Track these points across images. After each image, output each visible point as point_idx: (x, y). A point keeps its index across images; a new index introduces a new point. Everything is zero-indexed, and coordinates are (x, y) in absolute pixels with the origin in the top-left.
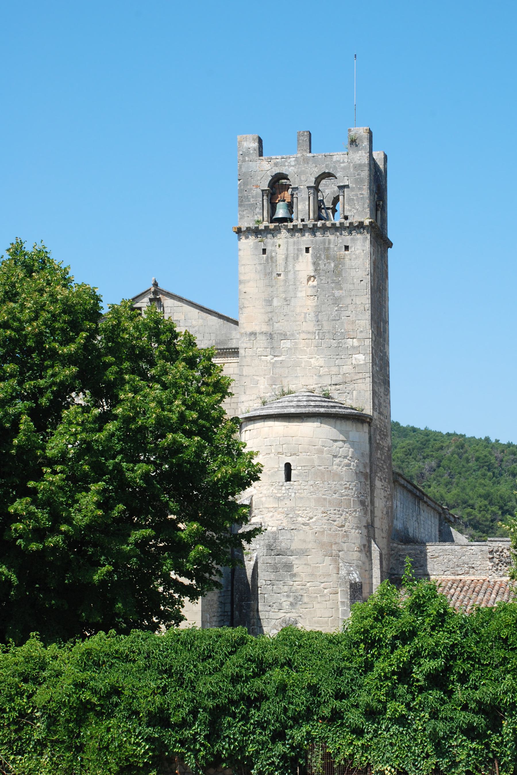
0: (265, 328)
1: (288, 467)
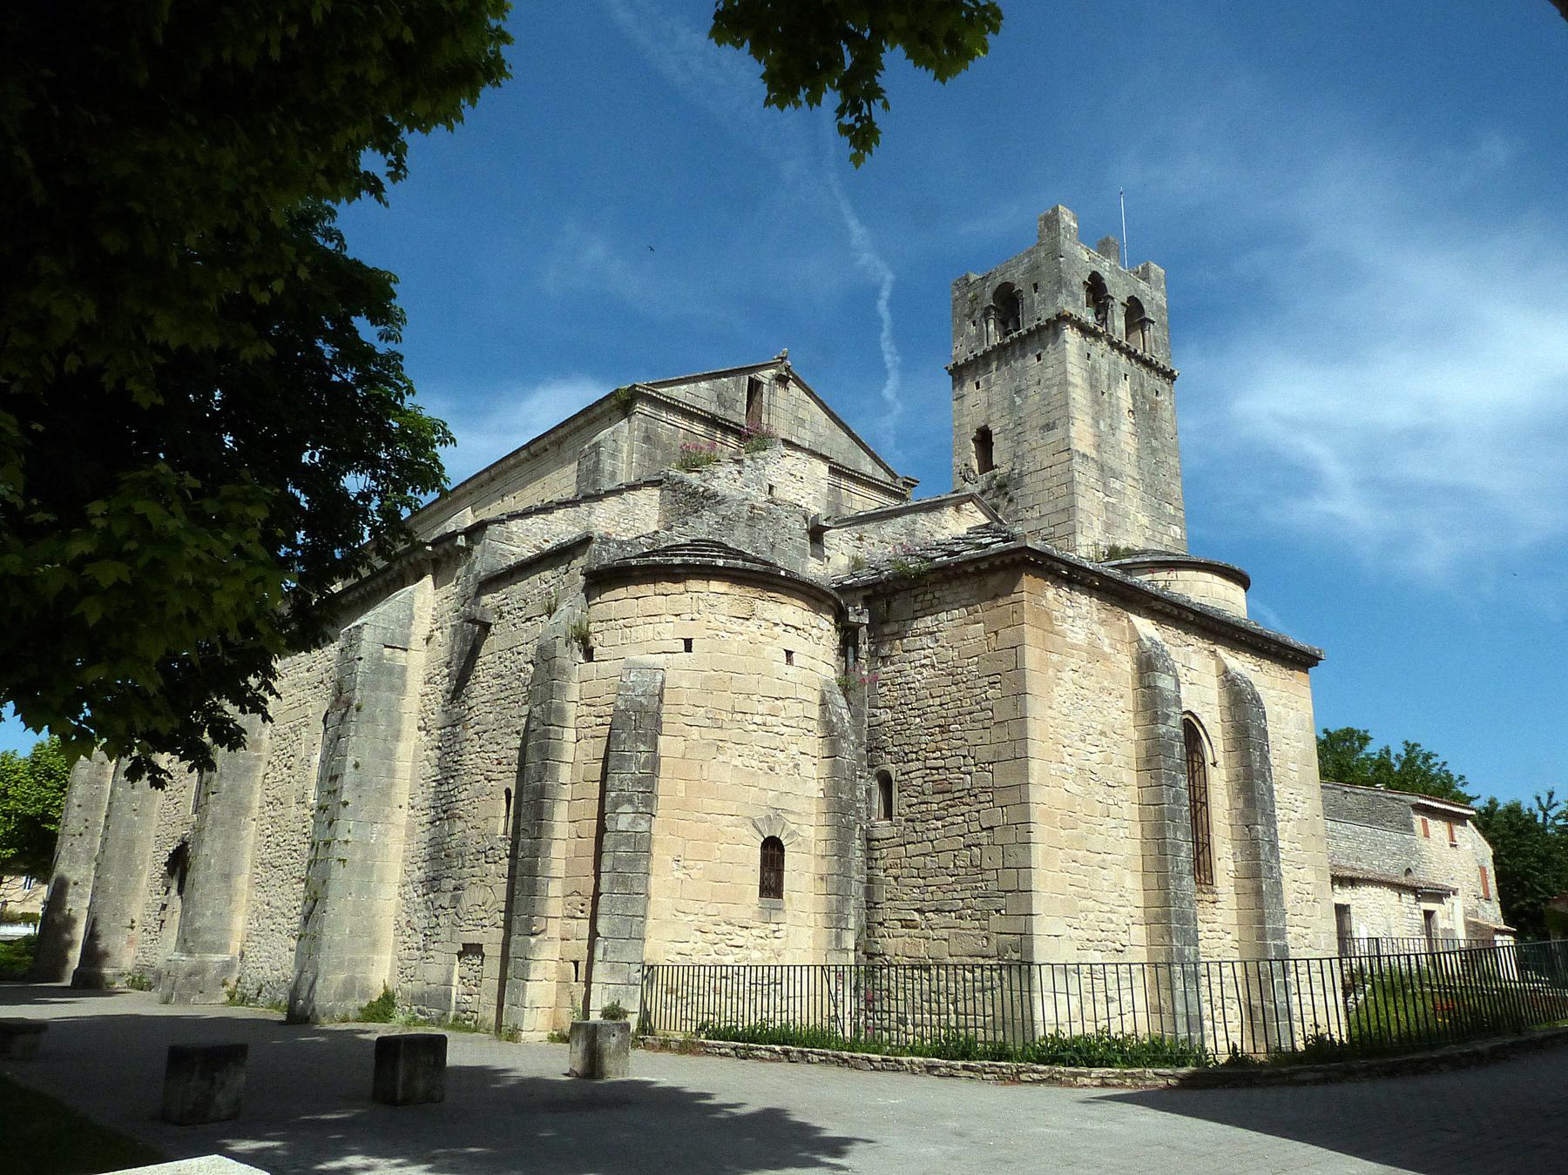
0: (1094, 454)
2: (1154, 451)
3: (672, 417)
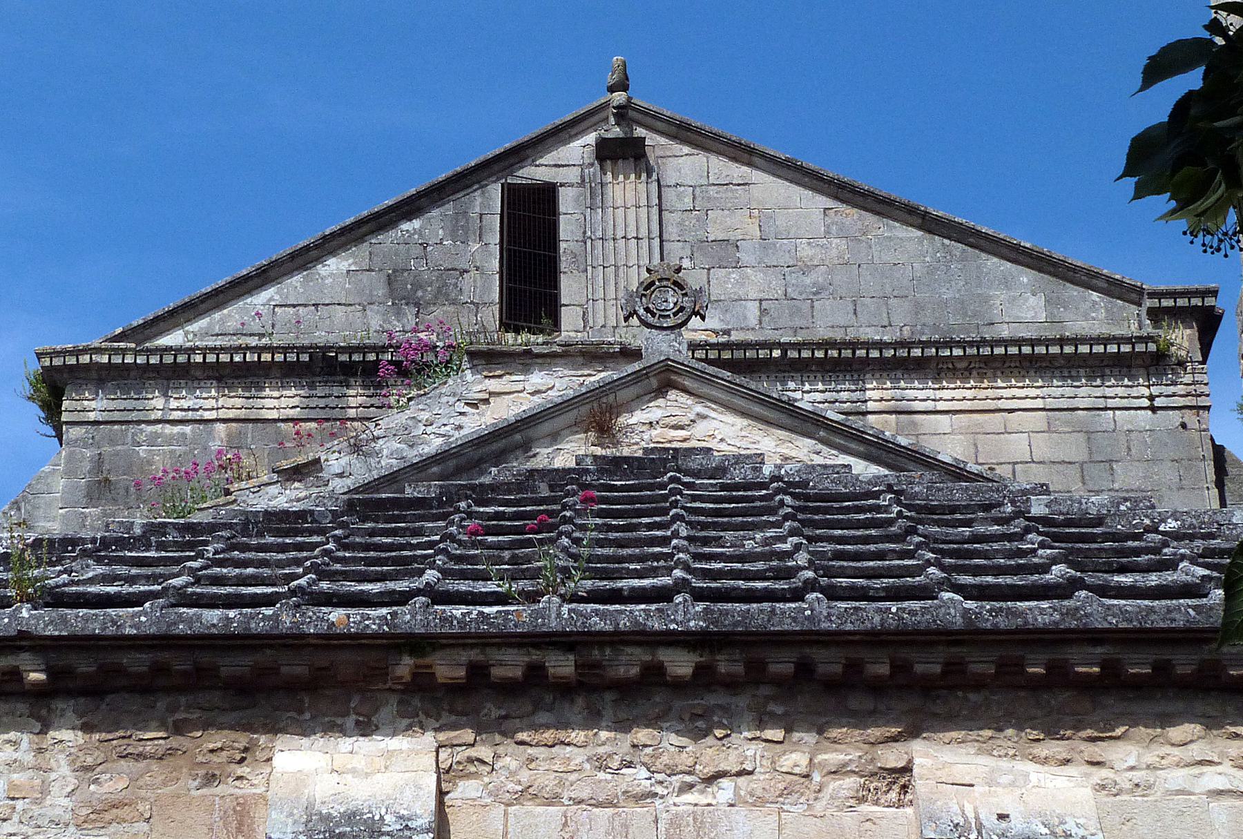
3: (183, 401)
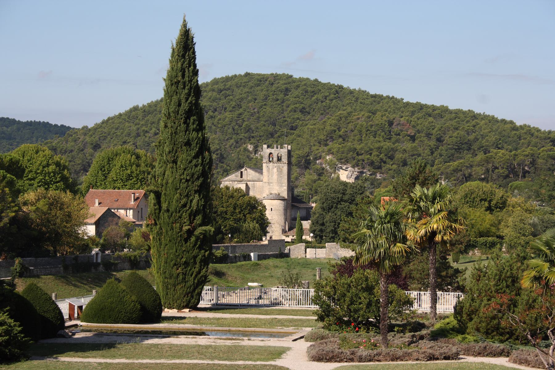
1: (272, 209)
2: (281, 177)
